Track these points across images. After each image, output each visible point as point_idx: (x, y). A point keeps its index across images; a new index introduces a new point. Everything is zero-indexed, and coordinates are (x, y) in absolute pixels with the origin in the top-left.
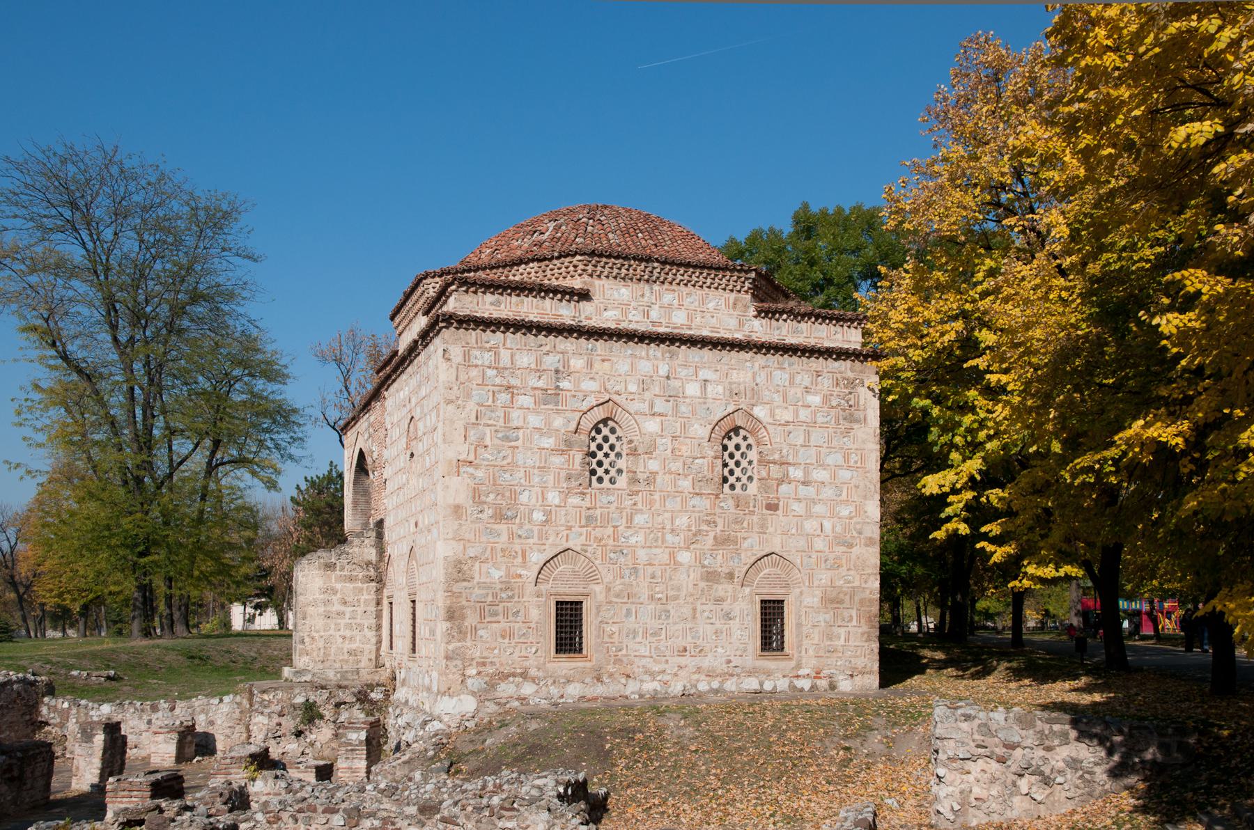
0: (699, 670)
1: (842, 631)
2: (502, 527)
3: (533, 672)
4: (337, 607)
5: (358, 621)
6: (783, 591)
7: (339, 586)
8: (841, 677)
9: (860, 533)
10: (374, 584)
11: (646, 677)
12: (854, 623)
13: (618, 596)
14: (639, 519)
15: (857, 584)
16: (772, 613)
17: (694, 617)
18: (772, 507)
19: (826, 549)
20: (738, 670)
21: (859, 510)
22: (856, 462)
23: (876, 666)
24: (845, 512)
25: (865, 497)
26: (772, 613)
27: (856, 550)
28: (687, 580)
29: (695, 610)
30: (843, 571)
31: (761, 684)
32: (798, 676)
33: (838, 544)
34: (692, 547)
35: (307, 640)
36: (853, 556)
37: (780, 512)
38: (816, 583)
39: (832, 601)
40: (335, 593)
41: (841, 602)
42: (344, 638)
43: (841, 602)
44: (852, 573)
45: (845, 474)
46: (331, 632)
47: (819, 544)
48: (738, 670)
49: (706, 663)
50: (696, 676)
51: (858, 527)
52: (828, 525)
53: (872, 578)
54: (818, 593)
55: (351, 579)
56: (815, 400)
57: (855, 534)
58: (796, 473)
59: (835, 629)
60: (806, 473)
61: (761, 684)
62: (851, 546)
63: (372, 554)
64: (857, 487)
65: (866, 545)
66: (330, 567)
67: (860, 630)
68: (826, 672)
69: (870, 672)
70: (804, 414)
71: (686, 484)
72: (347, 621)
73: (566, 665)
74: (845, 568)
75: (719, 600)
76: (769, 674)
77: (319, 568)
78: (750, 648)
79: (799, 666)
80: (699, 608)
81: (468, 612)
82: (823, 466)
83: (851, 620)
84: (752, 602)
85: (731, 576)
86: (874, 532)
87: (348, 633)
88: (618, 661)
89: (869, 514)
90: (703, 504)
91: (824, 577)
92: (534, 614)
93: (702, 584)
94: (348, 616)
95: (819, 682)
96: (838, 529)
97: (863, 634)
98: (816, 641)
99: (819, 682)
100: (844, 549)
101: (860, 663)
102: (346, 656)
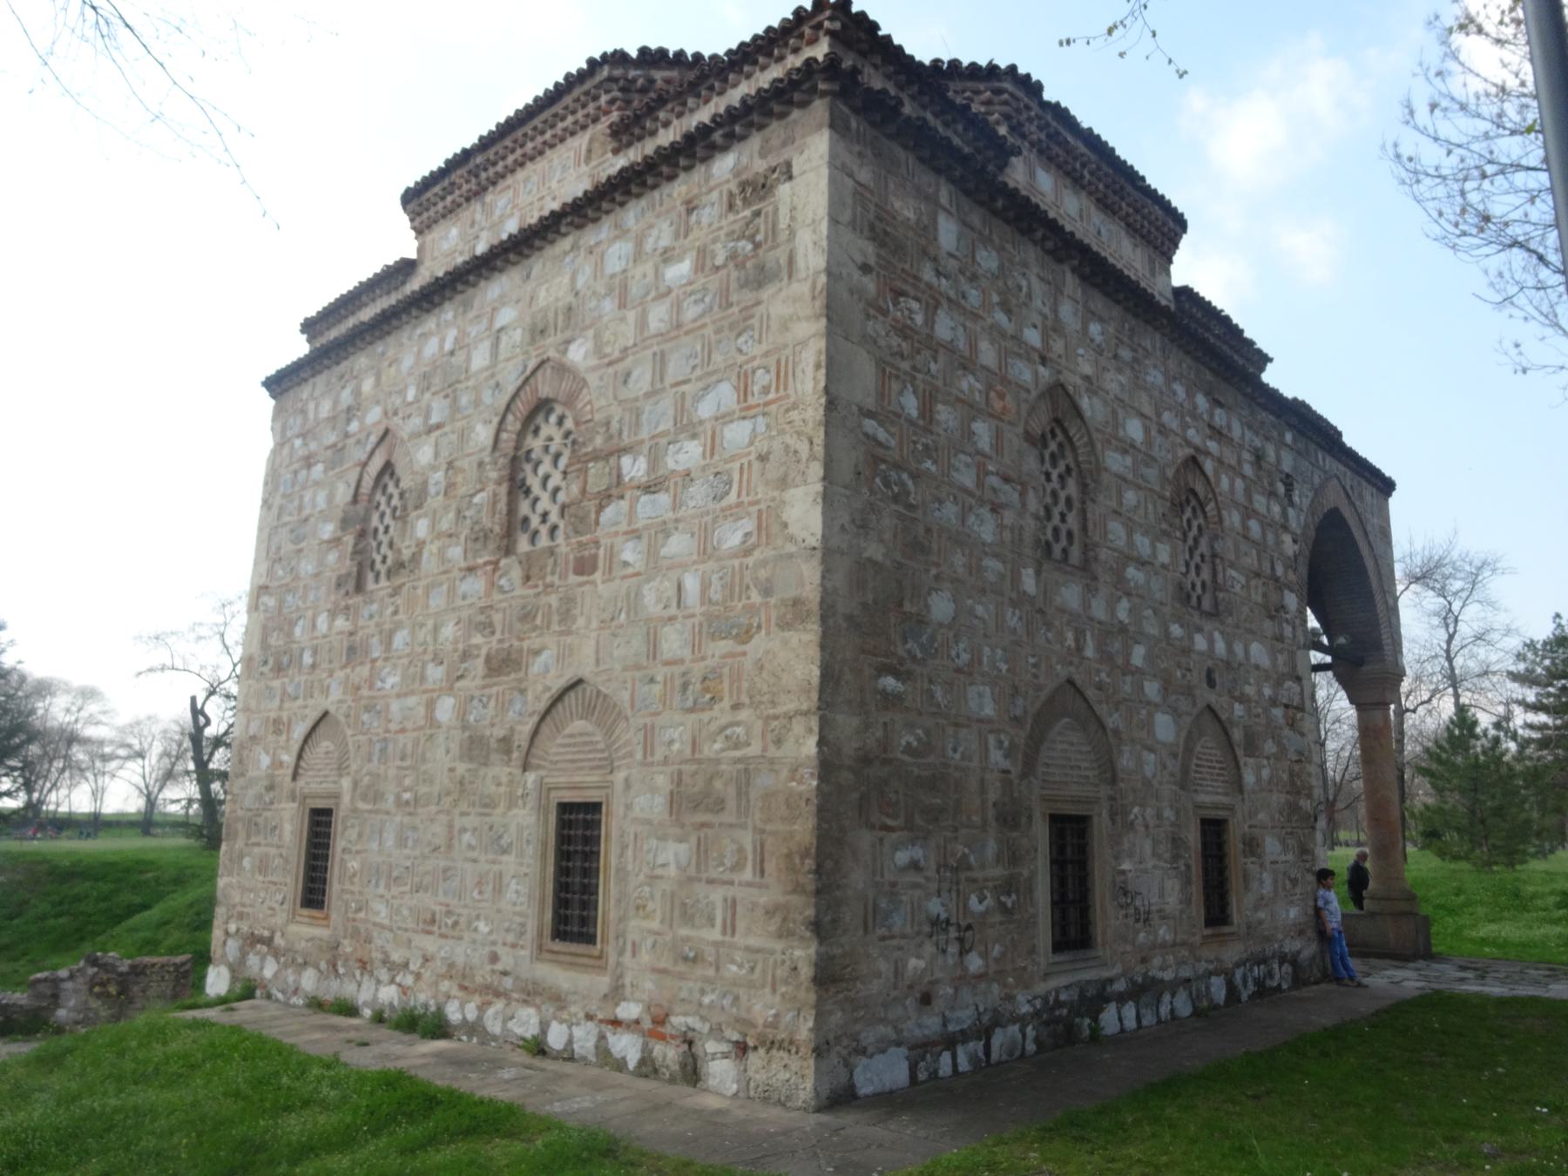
0: (450, 970)
1: (717, 895)
2: (276, 684)
3: (279, 941)
6: (594, 778)
8: (711, 1046)
9: (767, 591)
11: (384, 974)
12: (748, 874)
13: (364, 798)
14: (400, 639)
15: (754, 749)
16: (577, 833)
17: (450, 847)
18: (585, 566)
19: (686, 653)
20: (508, 982)
21: (769, 524)
22: (766, 390)
23: (805, 1029)
24: (732, 537)
25: (783, 483)
26: (577, 833)
27: (758, 645)
28: (443, 759)
29: (450, 826)
30: (720, 714)
31: (544, 1027)
32: (616, 1023)
33: (713, 637)
34: (458, 685)
36: (748, 663)
37: (598, 576)
38: (659, 754)
39: (693, 802)
41: (719, 806)
43: (719, 806)
44: (744, 715)
45: (737, 434)
47: (673, 642)
48: (508, 982)
49: (461, 952)
50: (445, 985)
51: (763, 574)
52: (691, 584)
53: (798, 726)
54: (662, 781)
56: (680, 270)
57: (756, 597)
58: (634, 468)
59: (701, 889)
60: (654, 461)
61: (544, 1027)
62: (745, 635)
64: (763, 458)
65: (784, 625)
67: (764, 899)
68: (678, 1021)
69: (788, 1045)
70: (658, 317)
71: (456, 552)
73: (305, 931)
74: (726, 703)
75: (489, 804)
76: (559, 1000)
78: (531, 926)
79: (616, 993)
80: (459, 822)
81: (240, 826)
82: (687, 427)
83: (738, 866)
84: (541, 809)
85: (506, 743)
86: (807, 579)
88: (355, 934)
89: (792, 530)
90: (474, 586)
91: (676, 733)
92: (288, 828)
93: (461, 768)
95: (658, 1049)
96: (716, 594)
97: (769, 913)
98: (655, 925)
99: (658, 1049)
100: (725, 646)
101: (762, 1008)
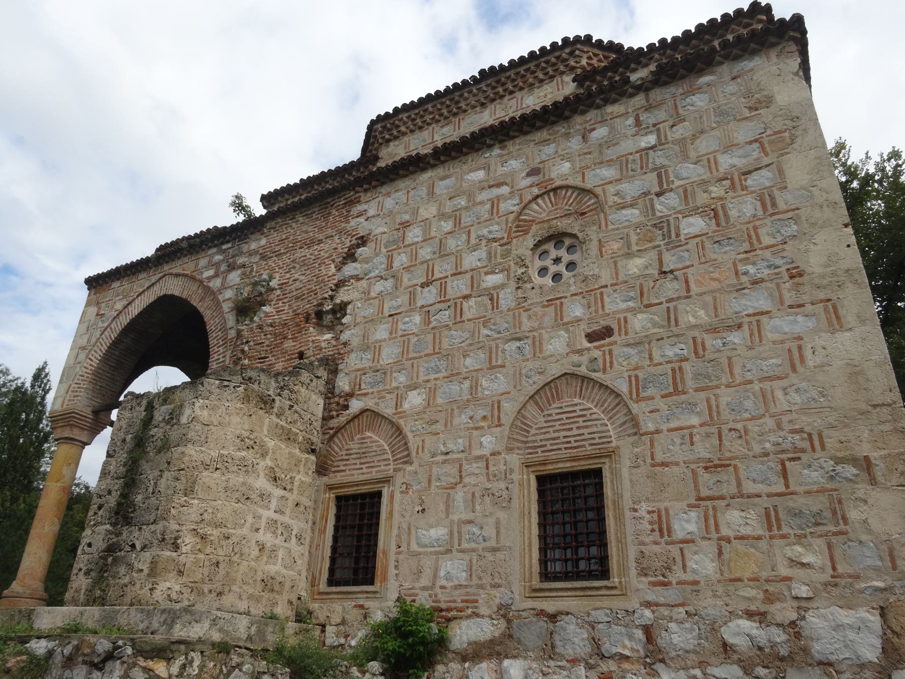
4: (261, 483)
5: (286, 519)
7: (271, 444)
10: (313, 458)
35: (188, 541)
40: (264, 456)
42: (262, 548)
46: (245, 531)
55: (288, 437)
63: (317, 405)
66: (266, 403)
72: (270, 514)
77: (246, 399)
87: (267, 538)
94: (274, 504)
102: (260, 586)
